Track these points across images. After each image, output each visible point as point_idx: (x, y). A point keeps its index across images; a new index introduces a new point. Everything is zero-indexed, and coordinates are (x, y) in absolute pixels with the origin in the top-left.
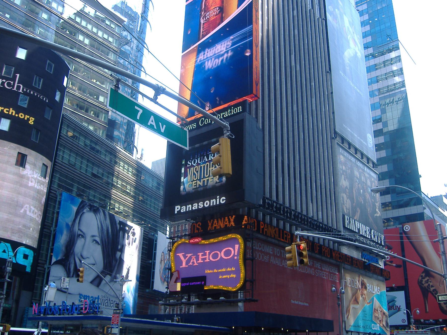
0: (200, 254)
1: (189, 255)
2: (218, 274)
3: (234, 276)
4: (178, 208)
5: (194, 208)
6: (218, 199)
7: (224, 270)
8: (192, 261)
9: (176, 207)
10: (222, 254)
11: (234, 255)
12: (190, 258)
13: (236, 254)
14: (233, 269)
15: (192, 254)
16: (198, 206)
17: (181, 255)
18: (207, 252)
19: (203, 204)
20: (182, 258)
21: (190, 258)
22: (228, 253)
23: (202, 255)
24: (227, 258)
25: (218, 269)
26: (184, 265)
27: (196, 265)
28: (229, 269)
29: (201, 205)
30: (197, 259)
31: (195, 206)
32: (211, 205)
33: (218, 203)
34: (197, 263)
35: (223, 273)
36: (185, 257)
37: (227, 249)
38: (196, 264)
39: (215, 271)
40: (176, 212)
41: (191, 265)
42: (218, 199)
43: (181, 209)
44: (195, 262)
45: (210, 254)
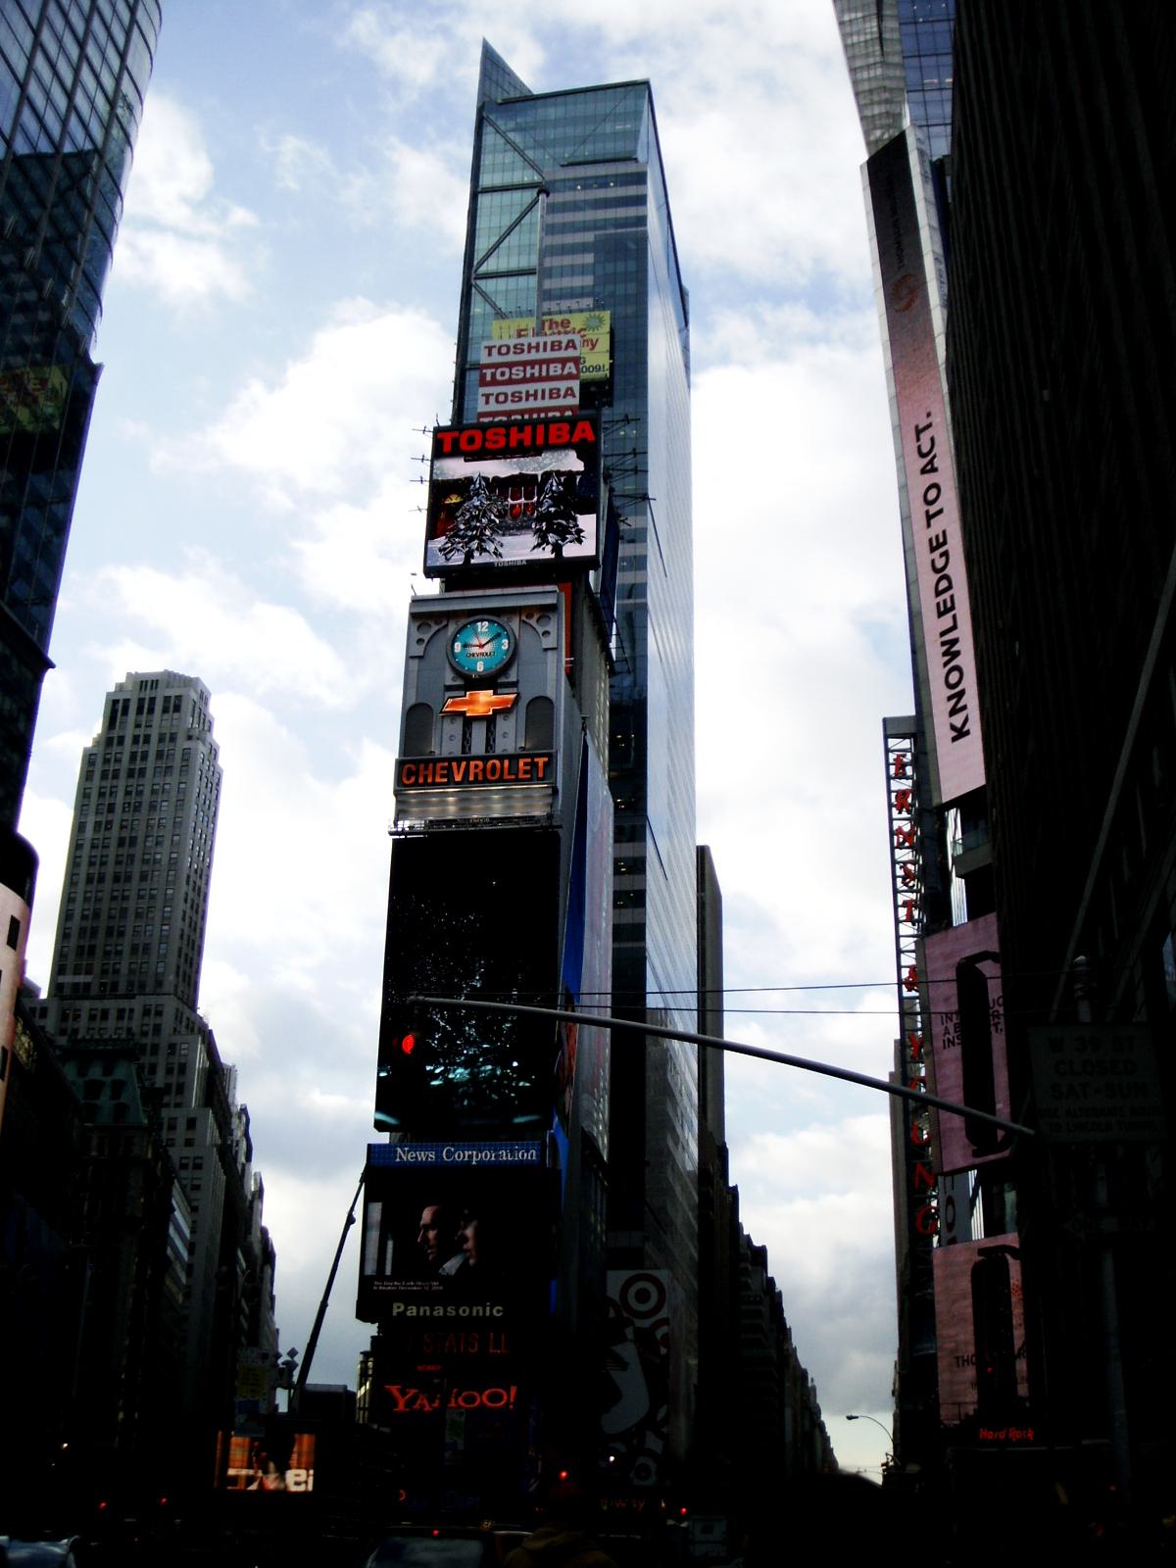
1: (413, 1391)
4: (399, 1307)
5: (435, 1313)
6: (488, 1308)
8: (419, 1402)
9: (395, 1306)
11: (508, 1403)
12: (413, 1400)
13: (512, 1400)
16: (445, 1311)
17: (394, 1389)
19: (457, 1311)
20: (397, 1394)
21: (413, 1400)
24: (490, 1404)
26: (401, 1406)
29: (451, 1311)
31: (439, 1311)
32: (474, 1314)
33: (488, 1313)
34: (430, 1406)
36: (403, 1393)
37: (494, 1390)
38: (427, 1408)
40: (395, 1314)
42: (488, 1308)
43: (406, 1310)
44: (427, 1406)
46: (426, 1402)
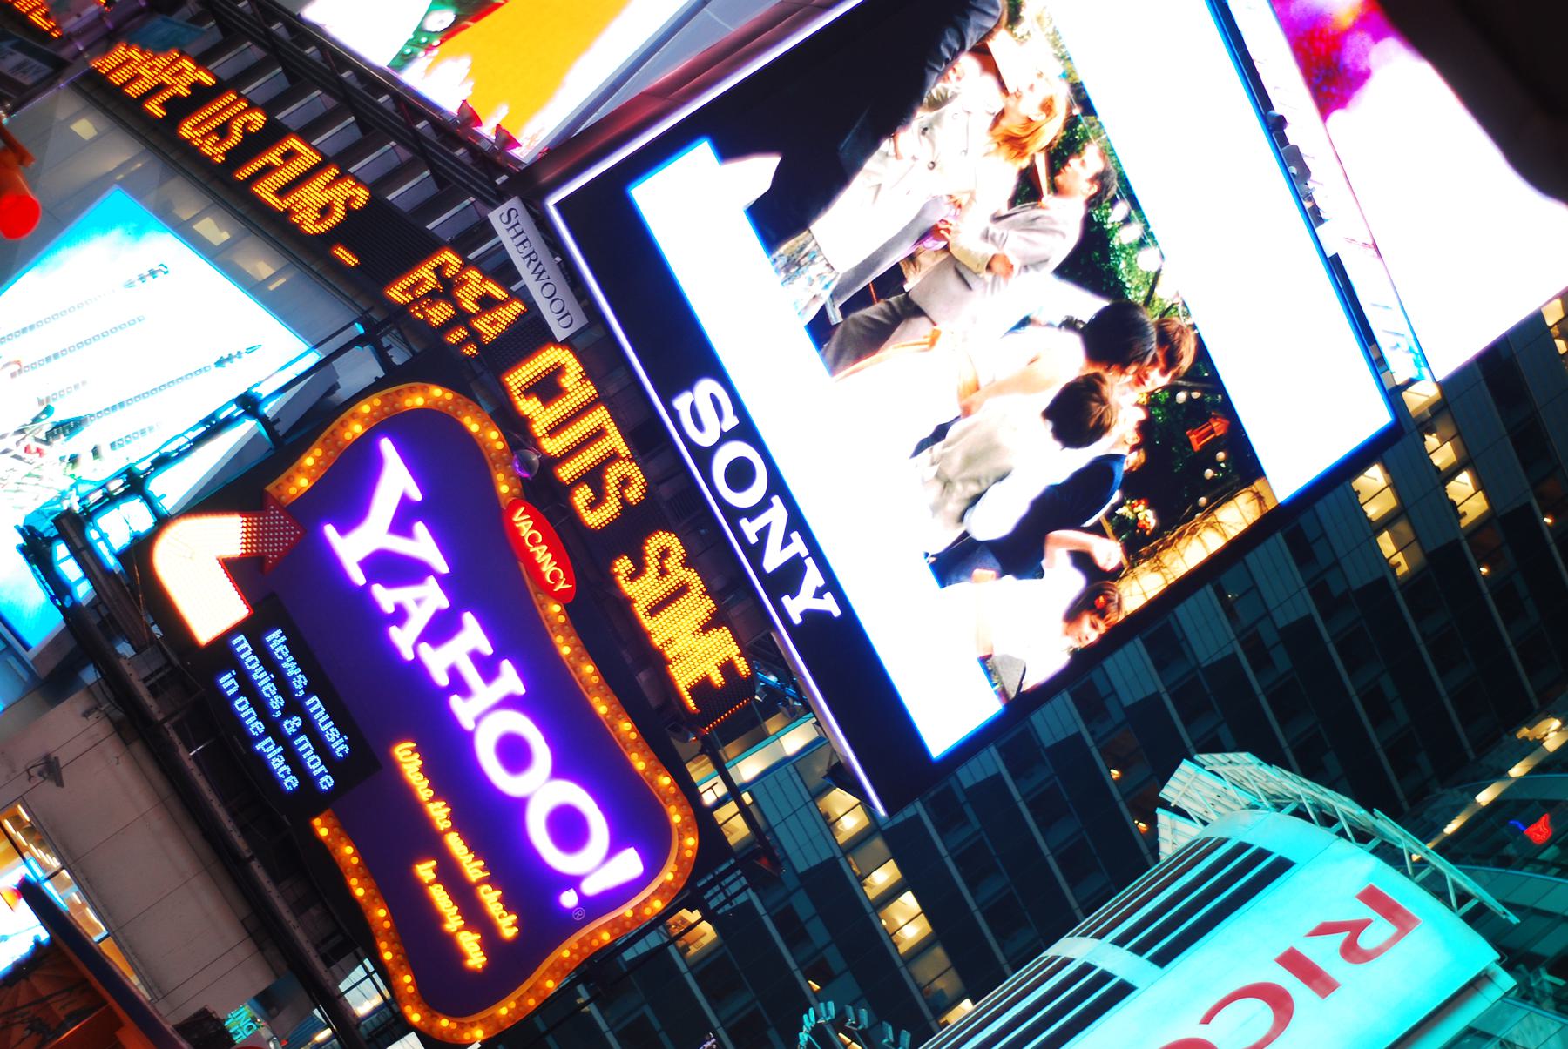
0: (473, 635)
2: (433, 845)
3: (476, 958)
7: (473, 869)
8: (404, 595)
10: (541, 790)
12: (412, 571)
14: (508, 926)
15: (442, 567)
17: (396, 481)
18: (510, 680)
20: (384, 504)
21: (412, 571)
22: (568, 827)
23: (476, 657)
25: (460, 822)
26: (351, 549)
27: (394, 650)
28: (491, 898)
30: (440, 630)
35: (450, 874)
36: (401, 524)
38: (403, 639)
39: (439, 813)
41: (374, 605)
45: (509, 702)
46: (419, 620)
